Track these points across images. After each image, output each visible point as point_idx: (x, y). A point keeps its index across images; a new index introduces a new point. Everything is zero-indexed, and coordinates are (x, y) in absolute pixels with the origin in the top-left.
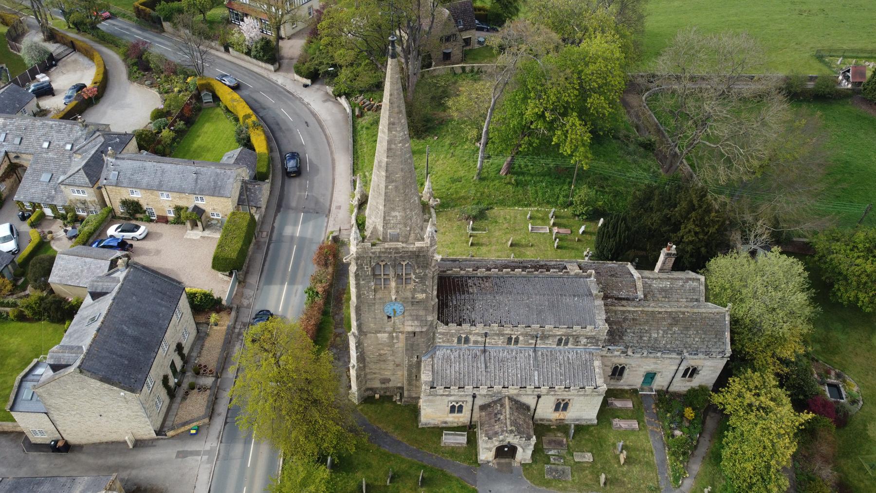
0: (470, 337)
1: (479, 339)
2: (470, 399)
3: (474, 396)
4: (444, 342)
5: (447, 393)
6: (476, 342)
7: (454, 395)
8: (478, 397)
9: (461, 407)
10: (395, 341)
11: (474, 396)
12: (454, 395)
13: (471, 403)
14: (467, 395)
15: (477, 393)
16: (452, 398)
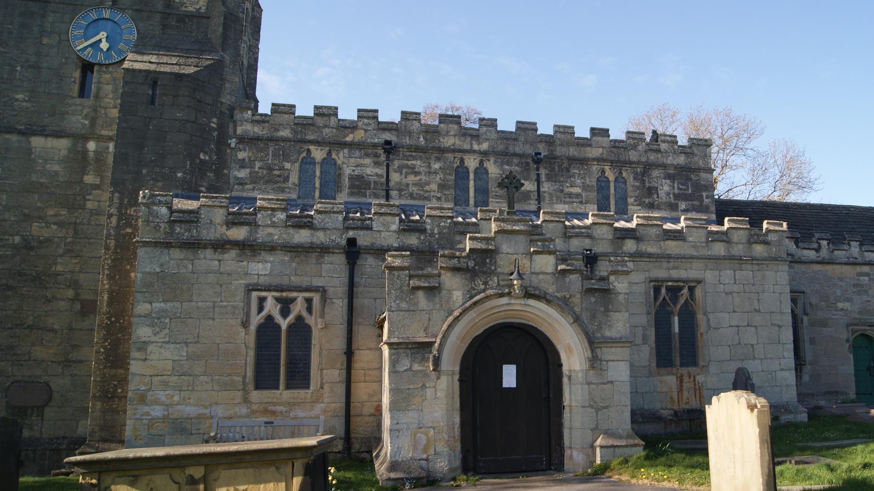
0: (340, 157)
1: (371, 170)
2: (332, 273)
3: (353, 252)
4: (255, 179)
5: (239, 233)
6: (359, 184)
7: (271, 248)
8: (368, 263)
9: (301, 331)
10: (89, 179)
11: (353, 252)
12: (271, 248)
13: (339, 306)
14: (324, 250)
15: (364, 239)
16: (261, 268)
